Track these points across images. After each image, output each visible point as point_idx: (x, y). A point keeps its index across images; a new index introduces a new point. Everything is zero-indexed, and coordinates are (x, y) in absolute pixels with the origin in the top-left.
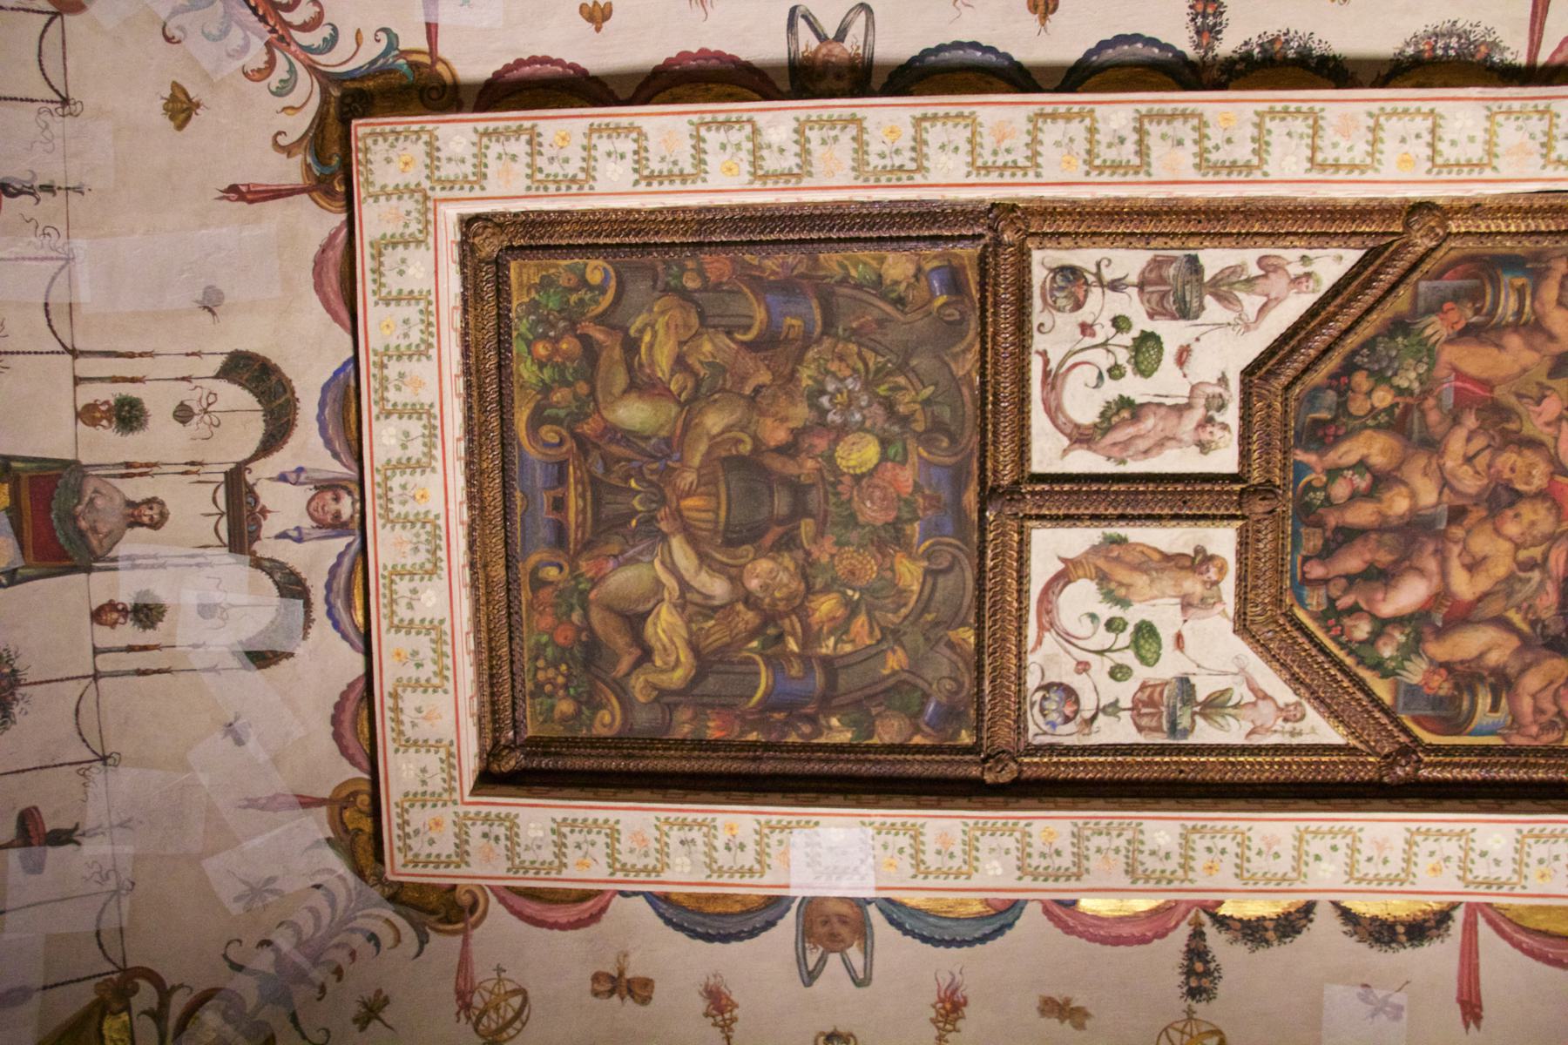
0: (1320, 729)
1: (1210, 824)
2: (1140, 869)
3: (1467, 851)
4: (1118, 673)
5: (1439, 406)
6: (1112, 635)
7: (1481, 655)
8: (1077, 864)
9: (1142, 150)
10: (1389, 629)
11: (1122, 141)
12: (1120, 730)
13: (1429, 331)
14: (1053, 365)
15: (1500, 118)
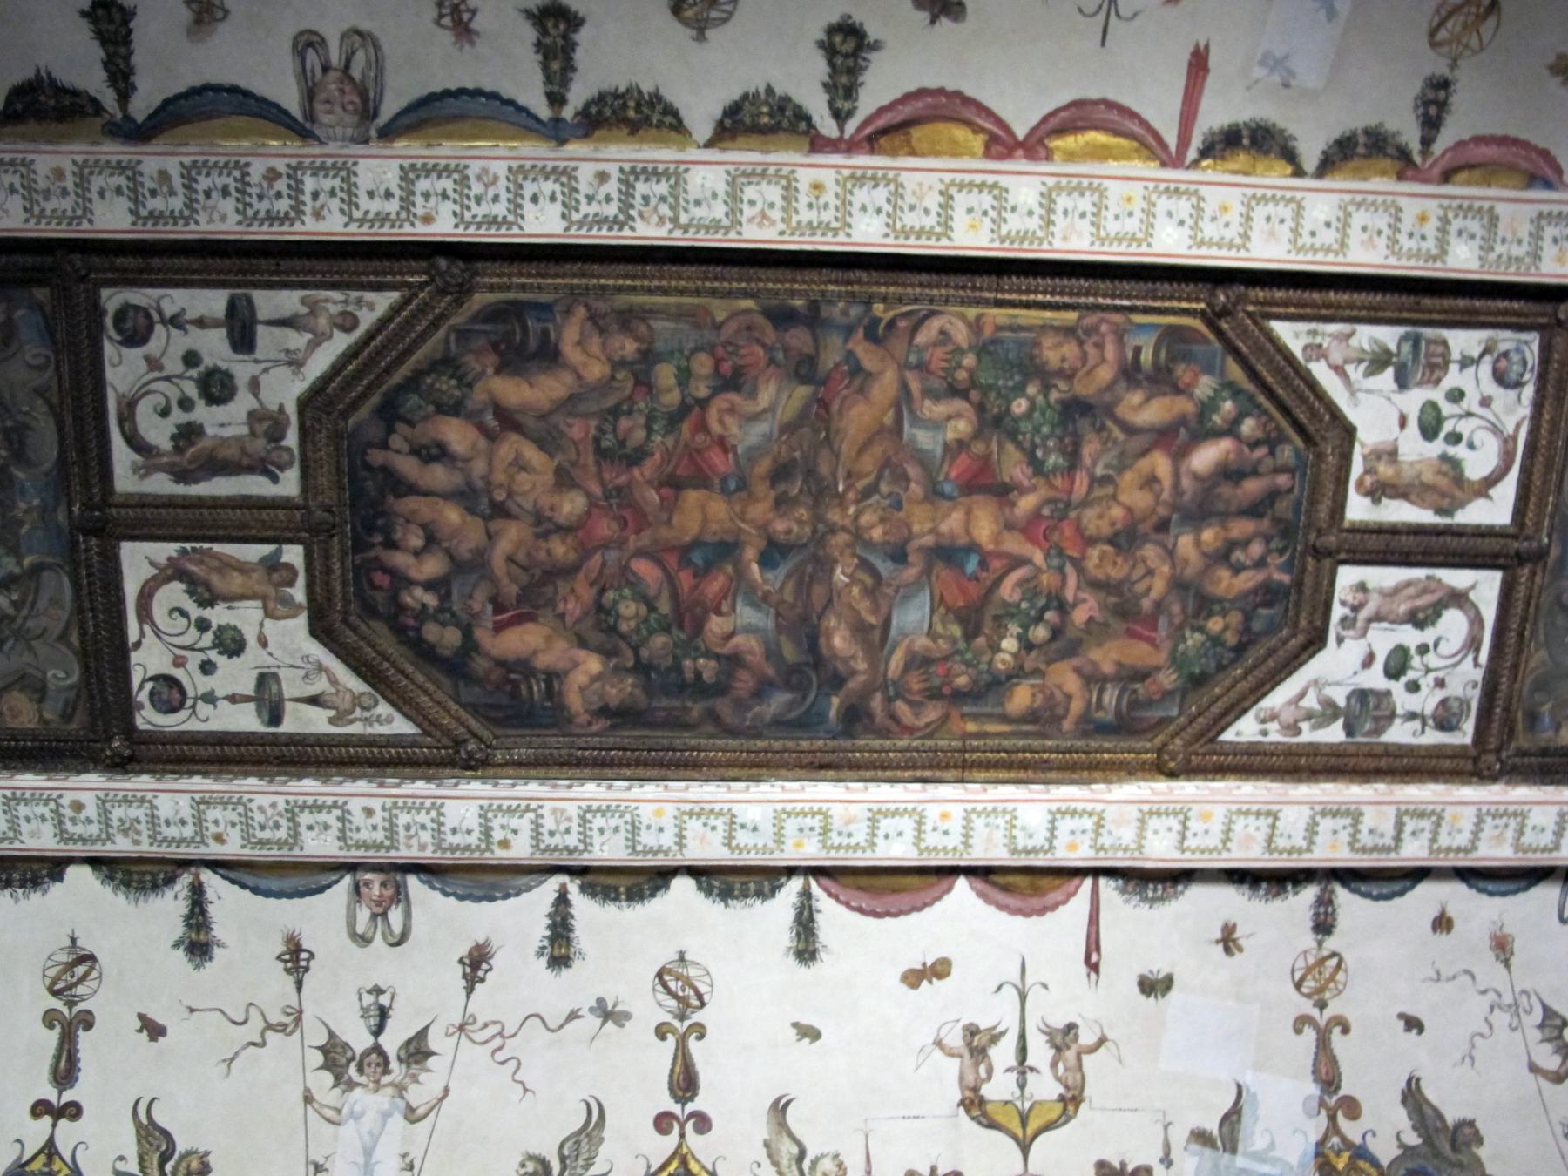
0: (1291, 334)
1: (1421, 263)
2: (1486, 220)
3: (1196, 227)
4: (1456, 396)
5: (1171, 617)
6: (1458, 429)
7: (1147, 400)
8: (1540, 228)
9: (1399, 826)
10: (1226, 427)
11: (1414, 833)
12: (1463, 341)
13: (1174, 677)
14: (1470, 657)
15: (1133, 846)
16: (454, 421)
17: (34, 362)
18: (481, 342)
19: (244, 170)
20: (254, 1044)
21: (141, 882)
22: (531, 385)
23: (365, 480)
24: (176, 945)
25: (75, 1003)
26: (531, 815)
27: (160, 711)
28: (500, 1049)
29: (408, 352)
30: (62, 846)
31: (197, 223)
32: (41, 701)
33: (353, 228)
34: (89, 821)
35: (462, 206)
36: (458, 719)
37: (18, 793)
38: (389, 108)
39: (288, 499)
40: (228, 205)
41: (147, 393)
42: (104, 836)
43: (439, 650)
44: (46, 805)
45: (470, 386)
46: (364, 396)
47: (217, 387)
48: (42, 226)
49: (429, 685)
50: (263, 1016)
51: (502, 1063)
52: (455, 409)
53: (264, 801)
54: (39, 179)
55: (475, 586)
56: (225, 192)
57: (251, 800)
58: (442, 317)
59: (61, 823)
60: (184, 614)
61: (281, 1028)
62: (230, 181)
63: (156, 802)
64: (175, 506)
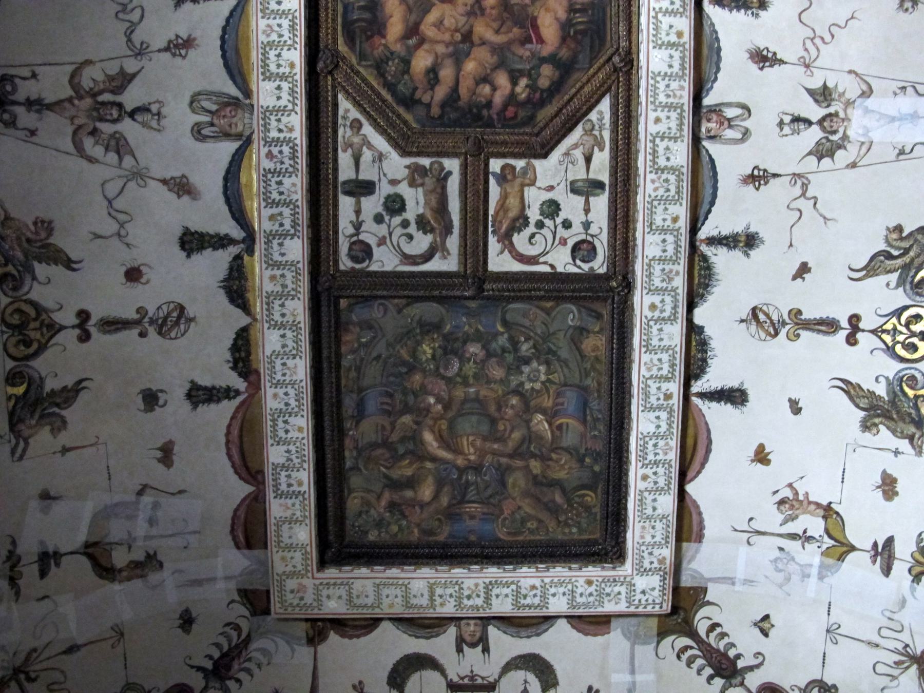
16: (413, 63)
17: (382, 313)
18: (366, 46)
19: (268, 171)
20: (815, 204)
21: (705, 278)
22: (391, 17)
23: (449, 118)
24: (748, 255)
25: (784, 321)
26: (660, 16)
27: (595, 257)
28: (822, 39)
29: (372, 88)
30: (679, 321)
31: (297, 200)
32: (588, 332)
33: (298, 109)
34: (663, 301)
35: (284, 46)
36: (599, 69)
37: (643, 343)
38: (233, 91)
39: (461, 165)
40: (287, 182)
41: (398, 245)
42: (673, 293)
43: (555, 79)
44: (651, 327)
45: (392, 53)
46: (399, 116)
47: (395, 205)
48: (302, 290)
49: (577, 86)
50: (795, 199)
51: (833, 36)
52: (406, 62)
53: (650, 187)
54: (276, 290)
55: (514, 54)
56: (280, 183)
57: (650, 196)
58: (352, 68)
59: (663, 319)
60: (533, 236)
61: (805, 187)
62: (274, 180)
63: (650, 257)
64: (466, 234)
